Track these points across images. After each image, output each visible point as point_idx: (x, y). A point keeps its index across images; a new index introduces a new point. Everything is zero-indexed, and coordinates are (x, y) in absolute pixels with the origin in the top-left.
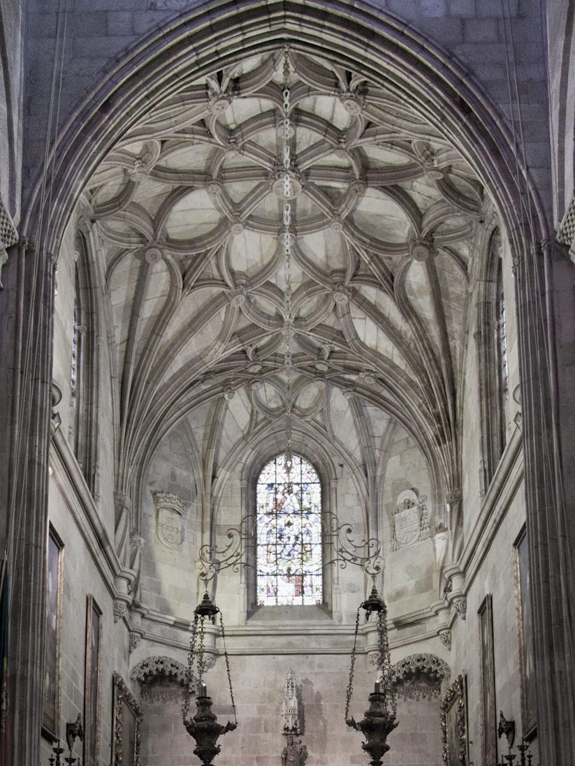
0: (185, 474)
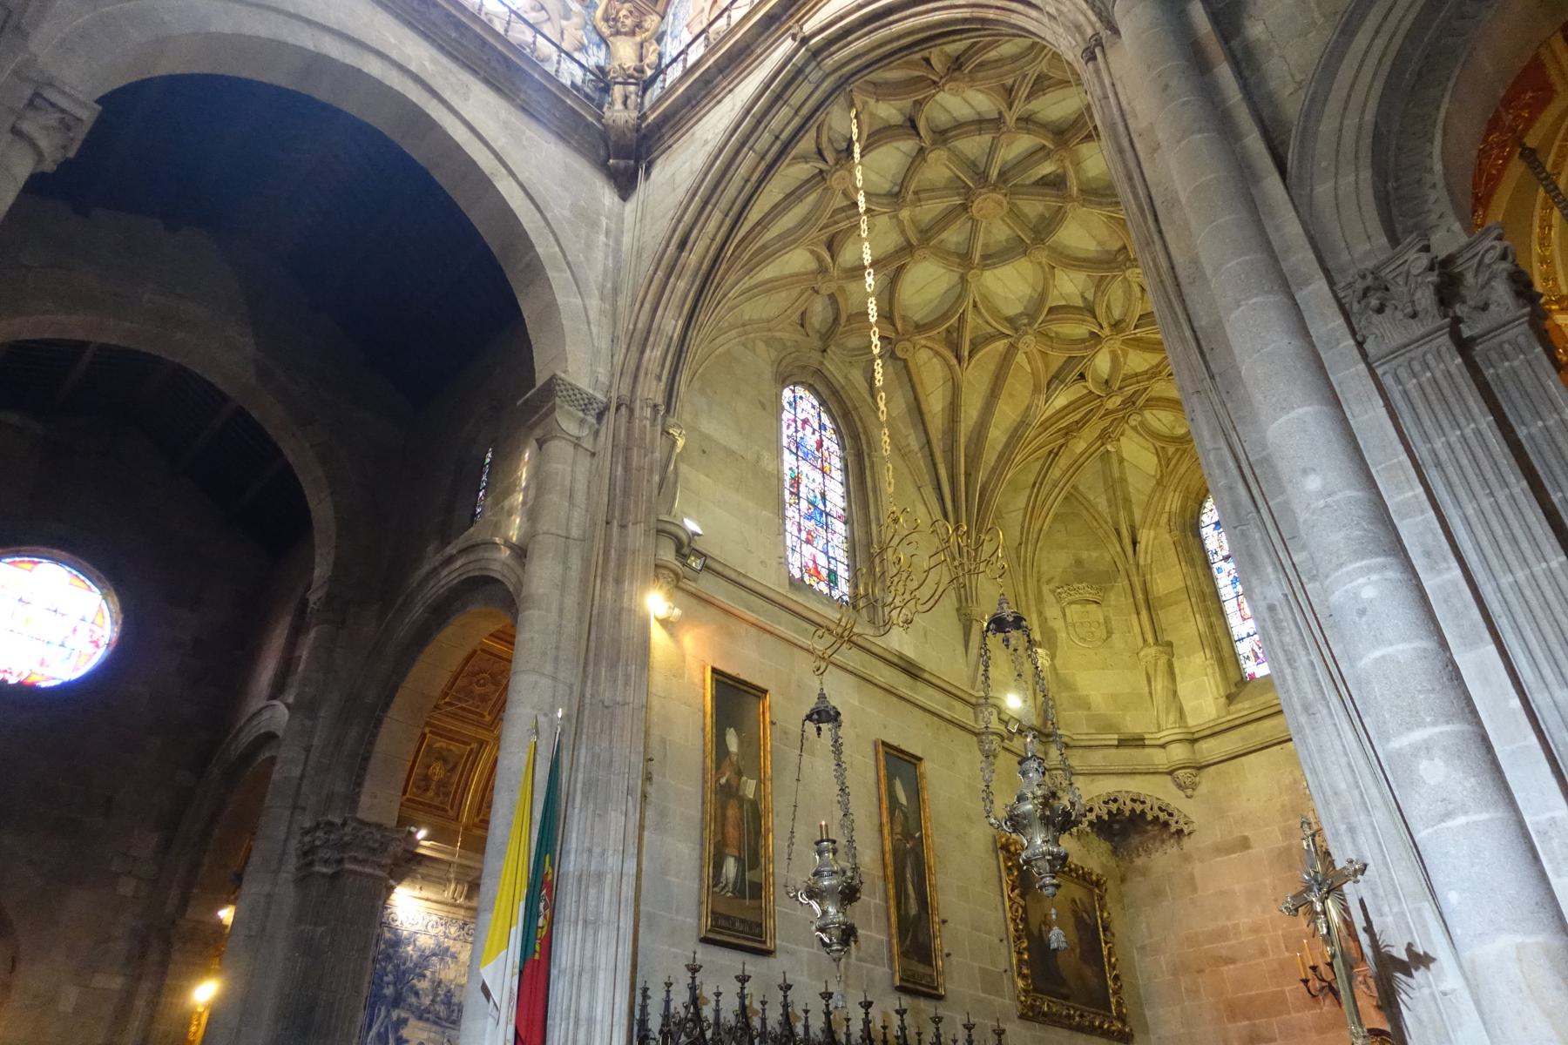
0: (1095, 554)
